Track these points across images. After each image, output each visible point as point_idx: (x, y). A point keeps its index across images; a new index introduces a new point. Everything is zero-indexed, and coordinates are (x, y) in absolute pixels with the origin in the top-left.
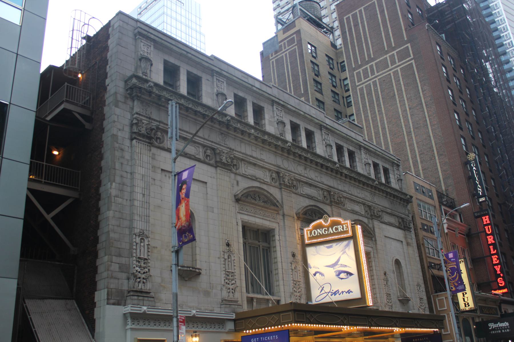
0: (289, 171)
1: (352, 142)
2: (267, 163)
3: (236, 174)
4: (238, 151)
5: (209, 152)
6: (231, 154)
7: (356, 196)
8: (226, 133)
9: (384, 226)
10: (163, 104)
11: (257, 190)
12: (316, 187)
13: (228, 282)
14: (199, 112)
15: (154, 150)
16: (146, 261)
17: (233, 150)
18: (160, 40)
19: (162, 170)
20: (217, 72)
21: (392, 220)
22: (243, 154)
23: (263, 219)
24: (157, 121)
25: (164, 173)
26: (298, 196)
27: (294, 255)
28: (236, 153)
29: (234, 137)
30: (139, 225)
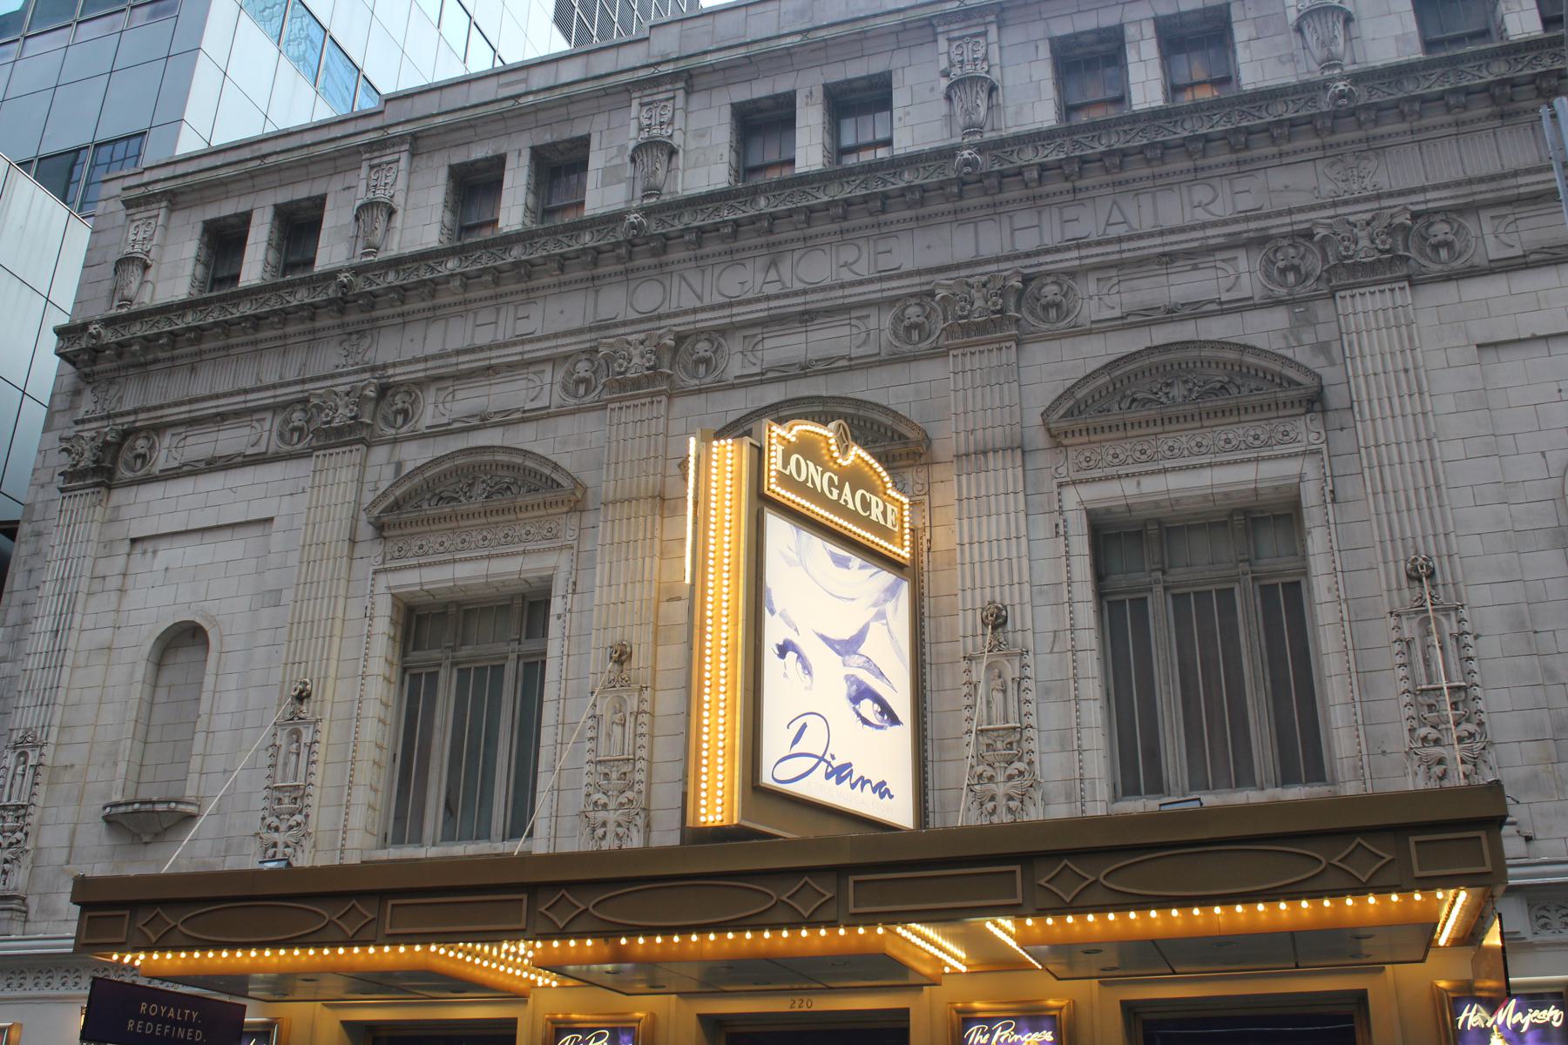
0: (659, 317)
2: (539, 339)
3: (395, 441)
4: (402, 363)
5: (297, 417)
6: (363, 388)
7: (1162, 233)
8: (366, 326)
9: (1476, 290)
10: (150, 357)
11: (459, 461)
12: (847, 309)
13: (276, 822)
14: (245, 318)
15: (118, 496)
16: (22, 812)
17: (385, 367)
18: (180, 181)
19: (134, 541)
20: (371, 146)
22: (426, 359)
23: (489, 557)
24: (128, 413)
25: (139, 547)
26: (719, 394)
27: (621, 656)
28: (398, 370)
29: (400, 320)
30: (25, 717)
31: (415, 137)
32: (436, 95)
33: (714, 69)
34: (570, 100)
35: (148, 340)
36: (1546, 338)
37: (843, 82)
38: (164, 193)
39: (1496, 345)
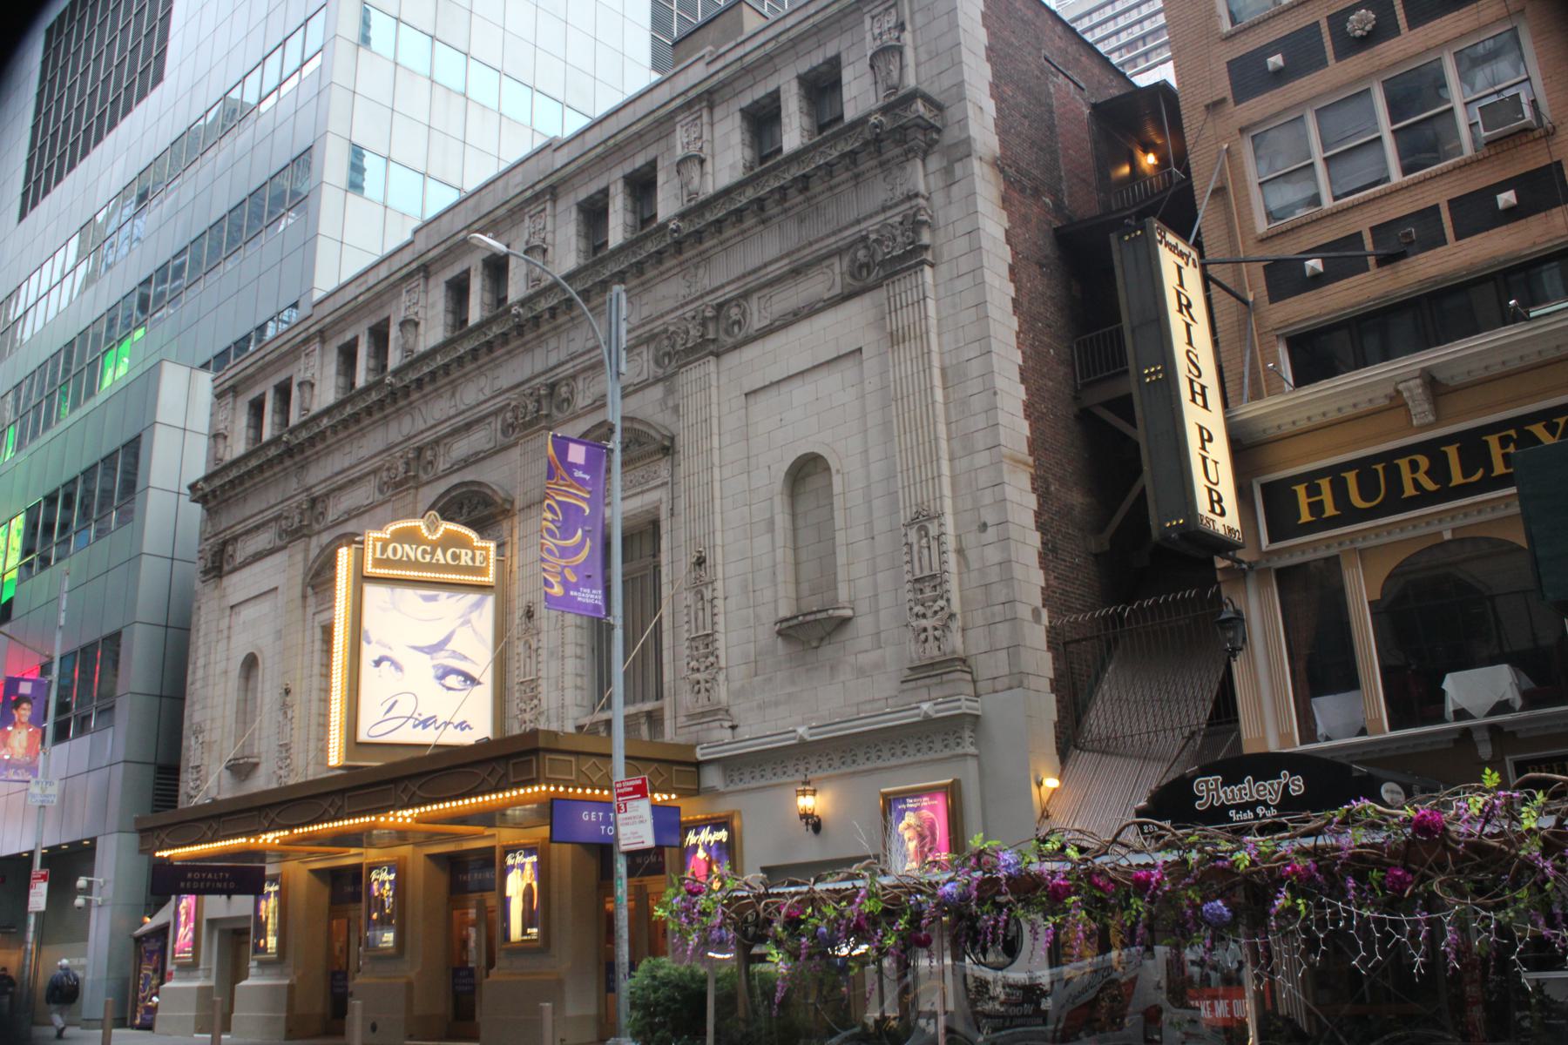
1: (639, 135)
21: (816, 286)
31: (321, 332)
32: (614, 118)
33: (435, 260)
34: (379, 295)
35: (222, 486)
36: (778, 382)
37: (810, 71)
38: (418, 269)
39: (755, 392)
